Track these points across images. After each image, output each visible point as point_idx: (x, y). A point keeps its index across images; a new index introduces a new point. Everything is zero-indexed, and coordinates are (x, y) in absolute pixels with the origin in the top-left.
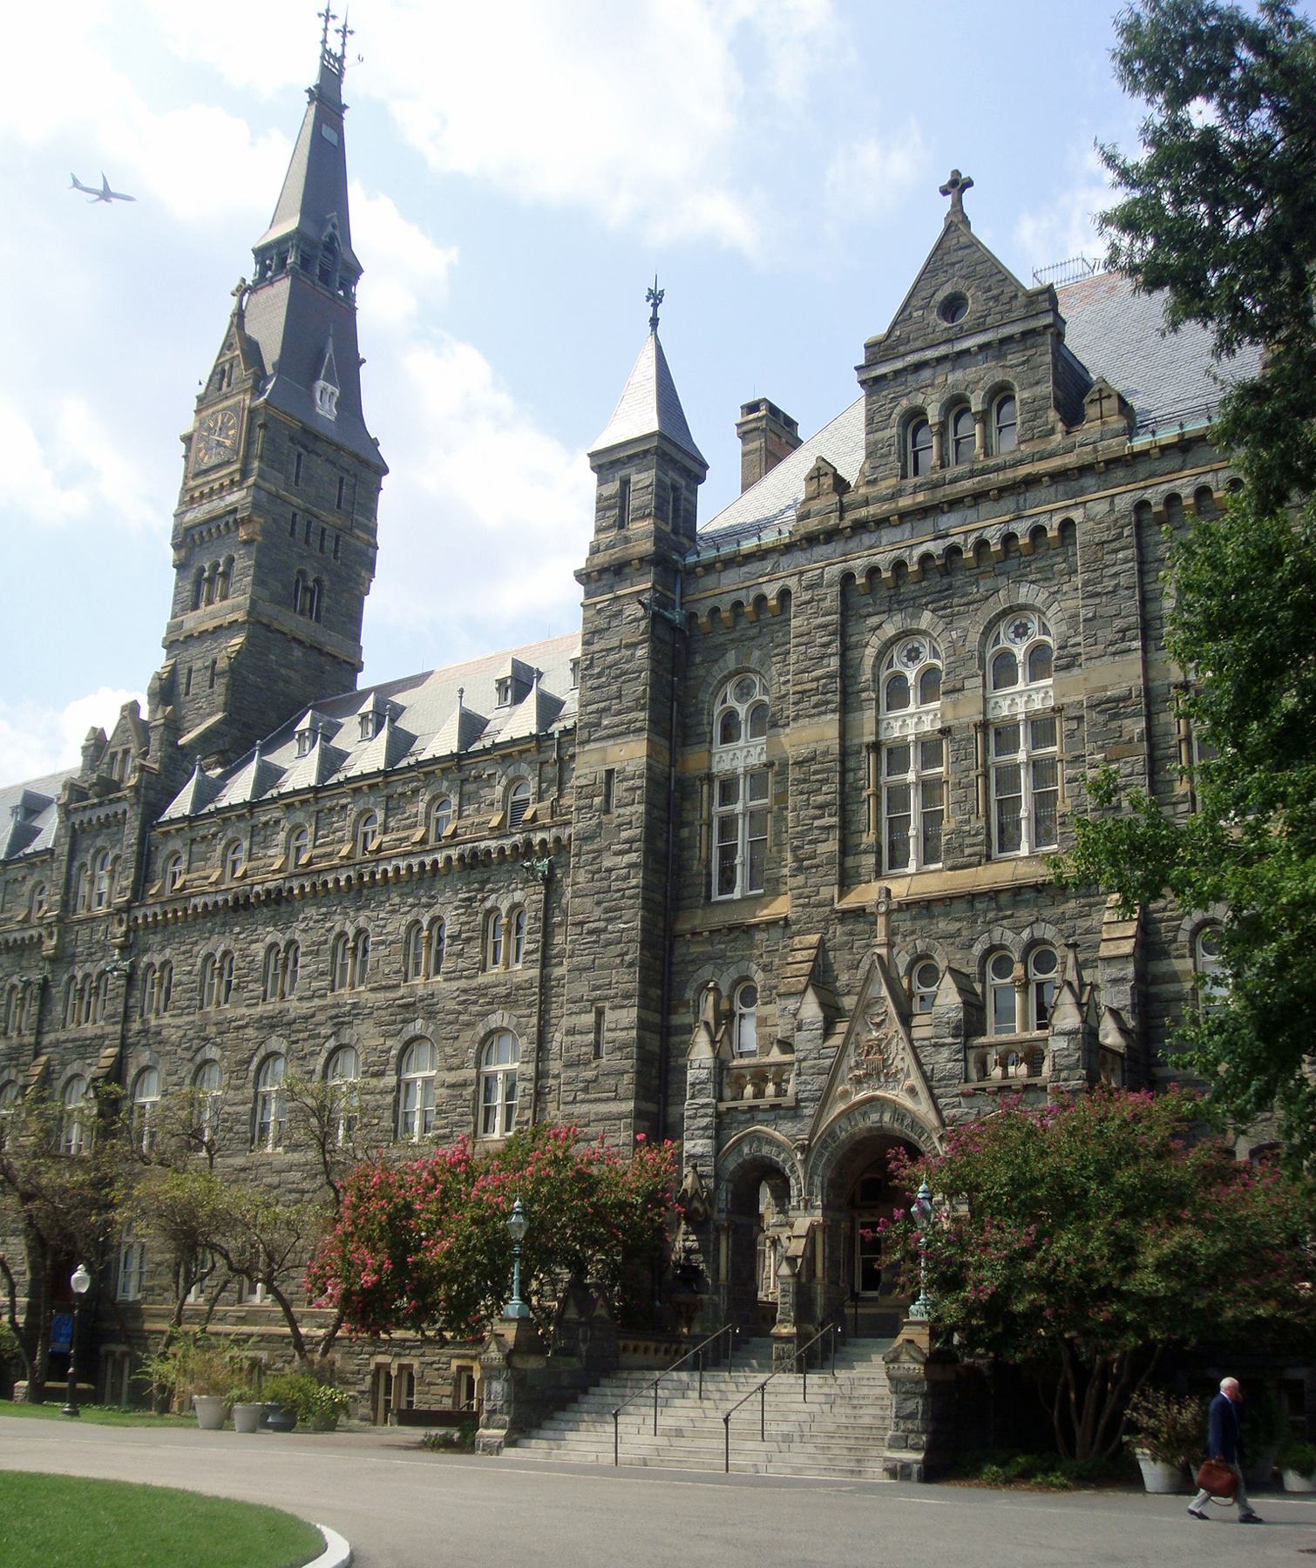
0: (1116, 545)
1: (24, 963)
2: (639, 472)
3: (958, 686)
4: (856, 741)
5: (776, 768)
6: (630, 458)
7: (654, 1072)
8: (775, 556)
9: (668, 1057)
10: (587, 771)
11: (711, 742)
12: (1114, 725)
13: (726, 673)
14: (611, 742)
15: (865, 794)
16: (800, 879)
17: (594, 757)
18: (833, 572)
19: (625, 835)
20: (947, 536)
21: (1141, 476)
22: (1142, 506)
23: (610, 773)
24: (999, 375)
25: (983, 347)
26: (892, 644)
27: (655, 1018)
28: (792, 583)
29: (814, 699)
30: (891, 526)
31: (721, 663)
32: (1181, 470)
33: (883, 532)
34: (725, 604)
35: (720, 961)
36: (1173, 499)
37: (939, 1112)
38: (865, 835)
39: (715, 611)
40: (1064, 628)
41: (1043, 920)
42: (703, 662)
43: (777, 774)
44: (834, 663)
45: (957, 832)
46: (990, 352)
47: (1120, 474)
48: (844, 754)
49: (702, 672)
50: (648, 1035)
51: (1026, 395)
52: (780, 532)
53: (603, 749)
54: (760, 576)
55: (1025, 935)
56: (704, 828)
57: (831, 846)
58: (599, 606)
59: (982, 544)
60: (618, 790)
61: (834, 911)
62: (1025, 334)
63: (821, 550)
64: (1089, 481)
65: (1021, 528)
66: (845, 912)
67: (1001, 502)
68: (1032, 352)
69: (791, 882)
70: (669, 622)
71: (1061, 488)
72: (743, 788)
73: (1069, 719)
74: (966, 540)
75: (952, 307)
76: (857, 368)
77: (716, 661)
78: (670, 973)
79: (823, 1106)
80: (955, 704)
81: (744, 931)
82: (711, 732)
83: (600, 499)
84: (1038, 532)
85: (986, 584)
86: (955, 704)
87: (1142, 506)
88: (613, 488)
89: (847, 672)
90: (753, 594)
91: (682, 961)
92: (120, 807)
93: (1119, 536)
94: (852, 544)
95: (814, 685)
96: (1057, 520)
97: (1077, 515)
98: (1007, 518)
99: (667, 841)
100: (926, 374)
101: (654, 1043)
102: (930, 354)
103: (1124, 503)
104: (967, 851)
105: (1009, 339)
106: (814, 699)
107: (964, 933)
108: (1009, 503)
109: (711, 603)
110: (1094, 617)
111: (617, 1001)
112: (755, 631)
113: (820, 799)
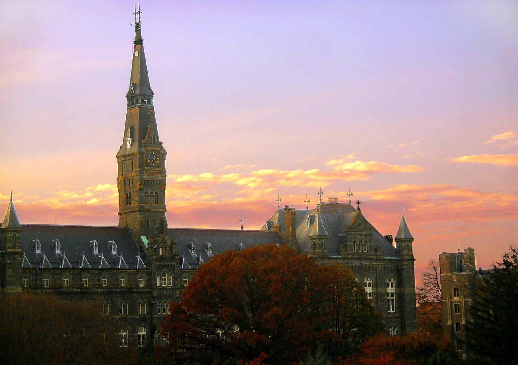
1: (143, 297)
24: (366, 240)
25: (365, 234)
47: (382, 262)
58: (321, 263)
65: (371, 266)
73: (375, 294)
75: (359, 225)
84: (373, 267)
92: (173, 263)
94: (349, 261)
96: (375, 266)
97: (377, 266)
100: (357, 236)
103: (383, 266)
105: (368, 235)
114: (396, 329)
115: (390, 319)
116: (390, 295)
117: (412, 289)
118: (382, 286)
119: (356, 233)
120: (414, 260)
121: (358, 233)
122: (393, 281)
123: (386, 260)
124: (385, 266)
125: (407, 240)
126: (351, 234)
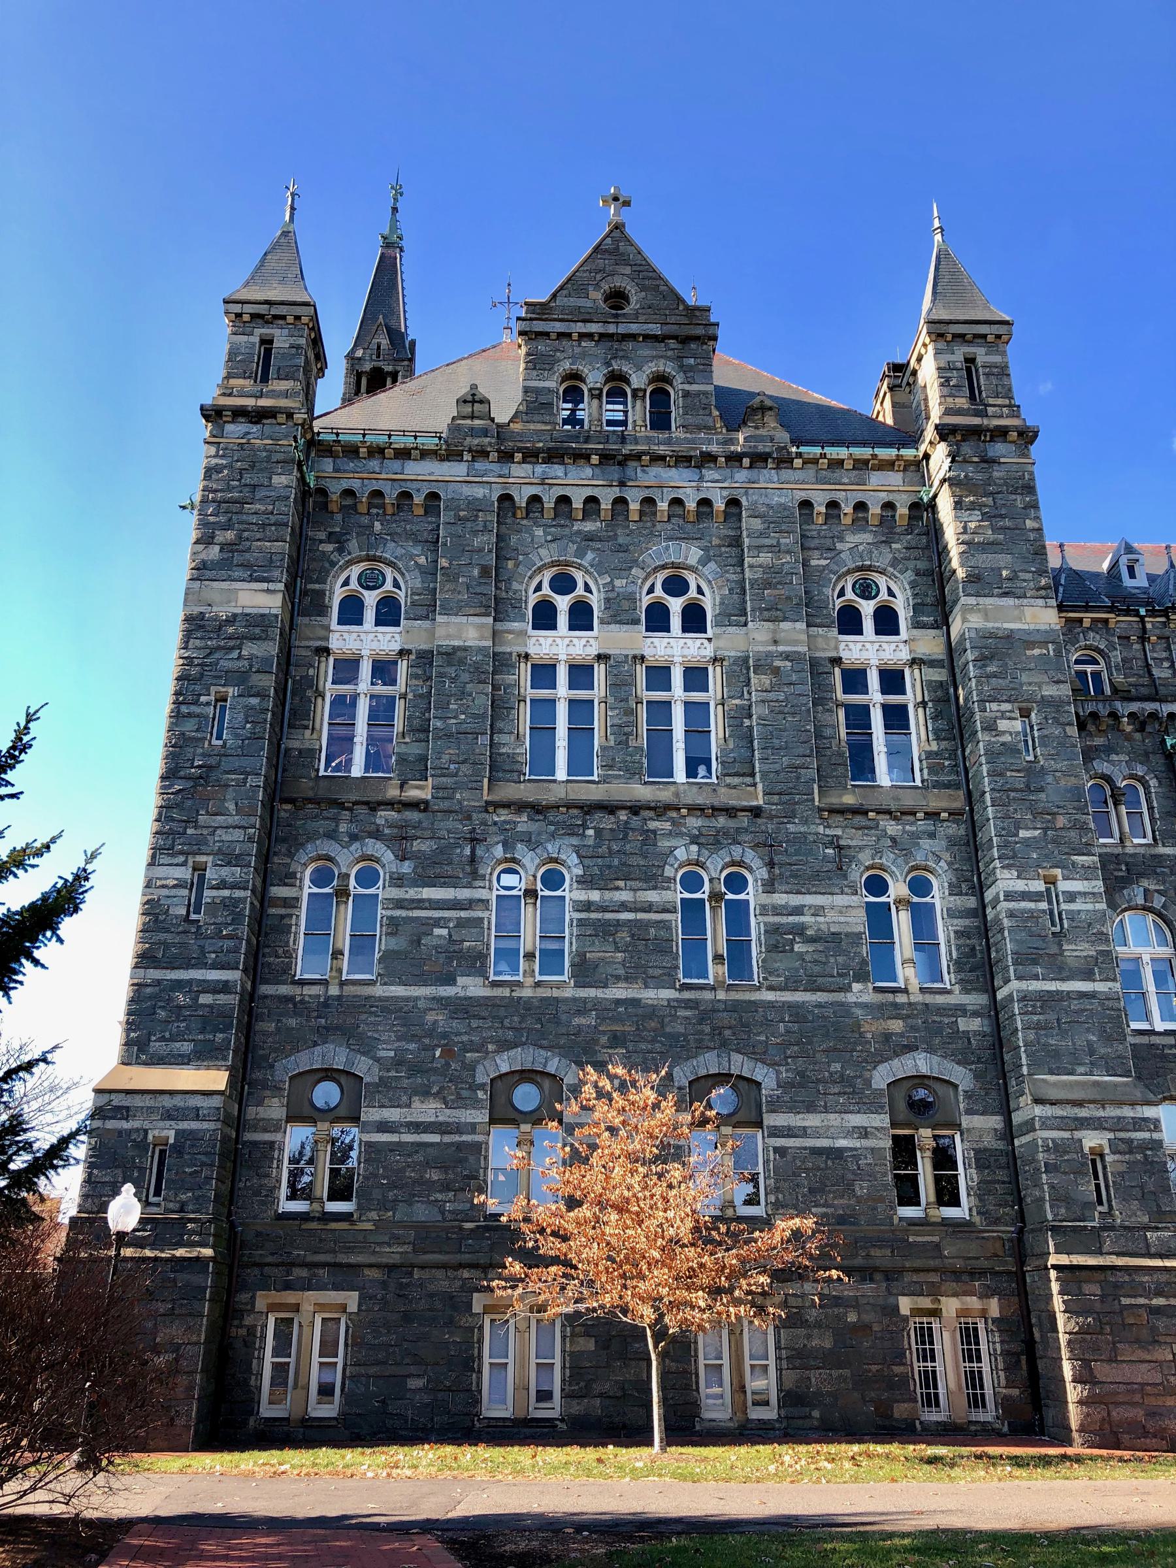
5: (412, 657)
48: (495, 654)
72: (366, 669)
120: (1028, 436)
121: (593, 328)
126: (547, 334)
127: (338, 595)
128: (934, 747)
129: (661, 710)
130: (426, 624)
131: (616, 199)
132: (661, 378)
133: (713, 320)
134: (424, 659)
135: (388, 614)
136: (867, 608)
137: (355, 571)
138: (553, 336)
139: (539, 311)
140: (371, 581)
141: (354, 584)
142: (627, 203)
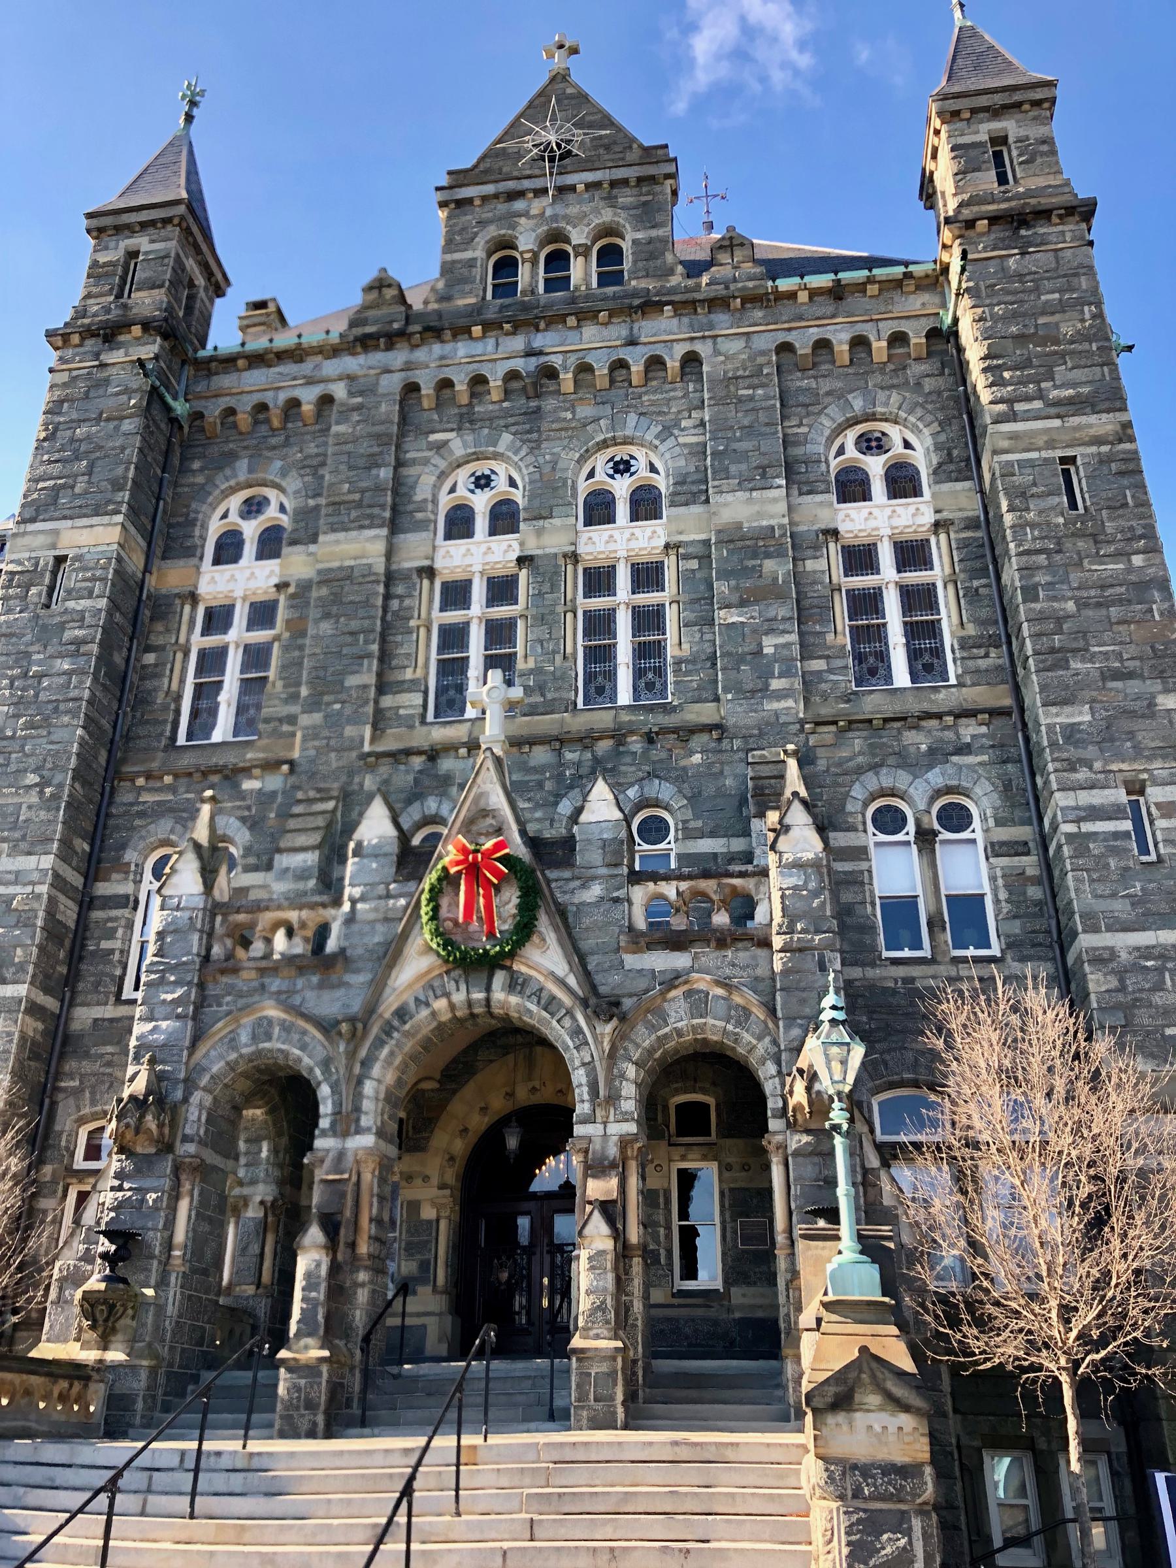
0: (756, 381)
2: (152, 241)
3: (544, 513)
4: (407, 565)
5: (291, 590)
6: (144, 225)
7: (62, 954)
8: (319, 358)
9: (85, 939)
10: (27, 555)
11: (201, 558)
12: (754, 562)
13: (232, 483)
14: (69, 523)
15: (413, 623)
16: (317, 718)
17: (41, 540)
18: (392, 384)
19: (68, 635)
20: (541, 353)
21: (784, 318)
22: (785, 348)
23: (60, 560)
24: (607, 216)
25: (589, 186)
26: (459, 466)
27: (77, 880)
28: (339, 391)
29: (354, 514)
30: (471, 338)
31: (228, 472)
32: (833, 316)
33: (460, 344)
34: (245, 406)
35: (185, 815)
36: (823, 345)
37: (586, 975)
38: (409, 671)
39: (231, 411)
40: (682, 463)
41: (657, 777)
42: (202, 470)
43: (293, 596)
44: (385, 474)
45: (537, 671)
46: (597, 194)
47: (759, 314)
48: (390, 578)
49: (200, 479)
50: (62, 898)
51: (639, 235)
52: (328, 332)
53: (56, 532)
54: (295, 379)
55: (632, 793)
56: (179, 656)
57: (367, 677)
58: (75, 373)
59: (584, 369)
60: (70, 579)
61: (364, 756)
62: (640, 180)
63: (378, 358)
64: (721, 318)
66: (379, 756)
67: (610, 327)
68: (650, 198)
69: (305, 720)
70: (168, 409)
71: (685, 320)
73: (686, 557)
74: (565, 361)
76: (438, 189)
77: (220, 468)
78: (105, 827)
79: (391, 966)
80: (539, 532)
81: (226, 778)
82: (203, 546)
83: (95, 264)
84: (655, 363)
85: (585, 411)
86: (539, 532)
87: (785, 348)
88: (114, 254)
89: (400, 489)
90: (283, 396)
91: (126, 813)
93: (758, 372)
95: (357, 496)
96: (680, 350)
98: (618, 343)
99: (128, 660)
100: (519, 205)
101: (68, 913)
102: (526, 184)
103: (766, 342)
104: (549, 696)
105: (625, 182)
106: (354, 514)
107: (548, 786)
108: (618, 331)
109: (225, 402)
110: (726, 450)
111: (23, 846)
112: (274, 441)
113: (355, 625)
114: (976, 831)
115: (857, 742)
116: (886, 556)
117: (1078, 428)
118: (756, 480)
119: (511, 185)
122: (907, 445)
123: (792, 295)
124: (790, 338)
125: (983, 101)
126: (469, 201)
127: (215, 529)
128: (971, 630)
129: (599, 624)
130: (312, 548)
131: (561, 47)
132: (610, 231)
133: (672, 155)
134: (300, 593)
135: (270, 545)
136: (875, 466)
137: (235, 502)
138: (477, 202)
139: (459, 178)
140: (253, 508)
141: (234, 517)
142: (574, 51)
